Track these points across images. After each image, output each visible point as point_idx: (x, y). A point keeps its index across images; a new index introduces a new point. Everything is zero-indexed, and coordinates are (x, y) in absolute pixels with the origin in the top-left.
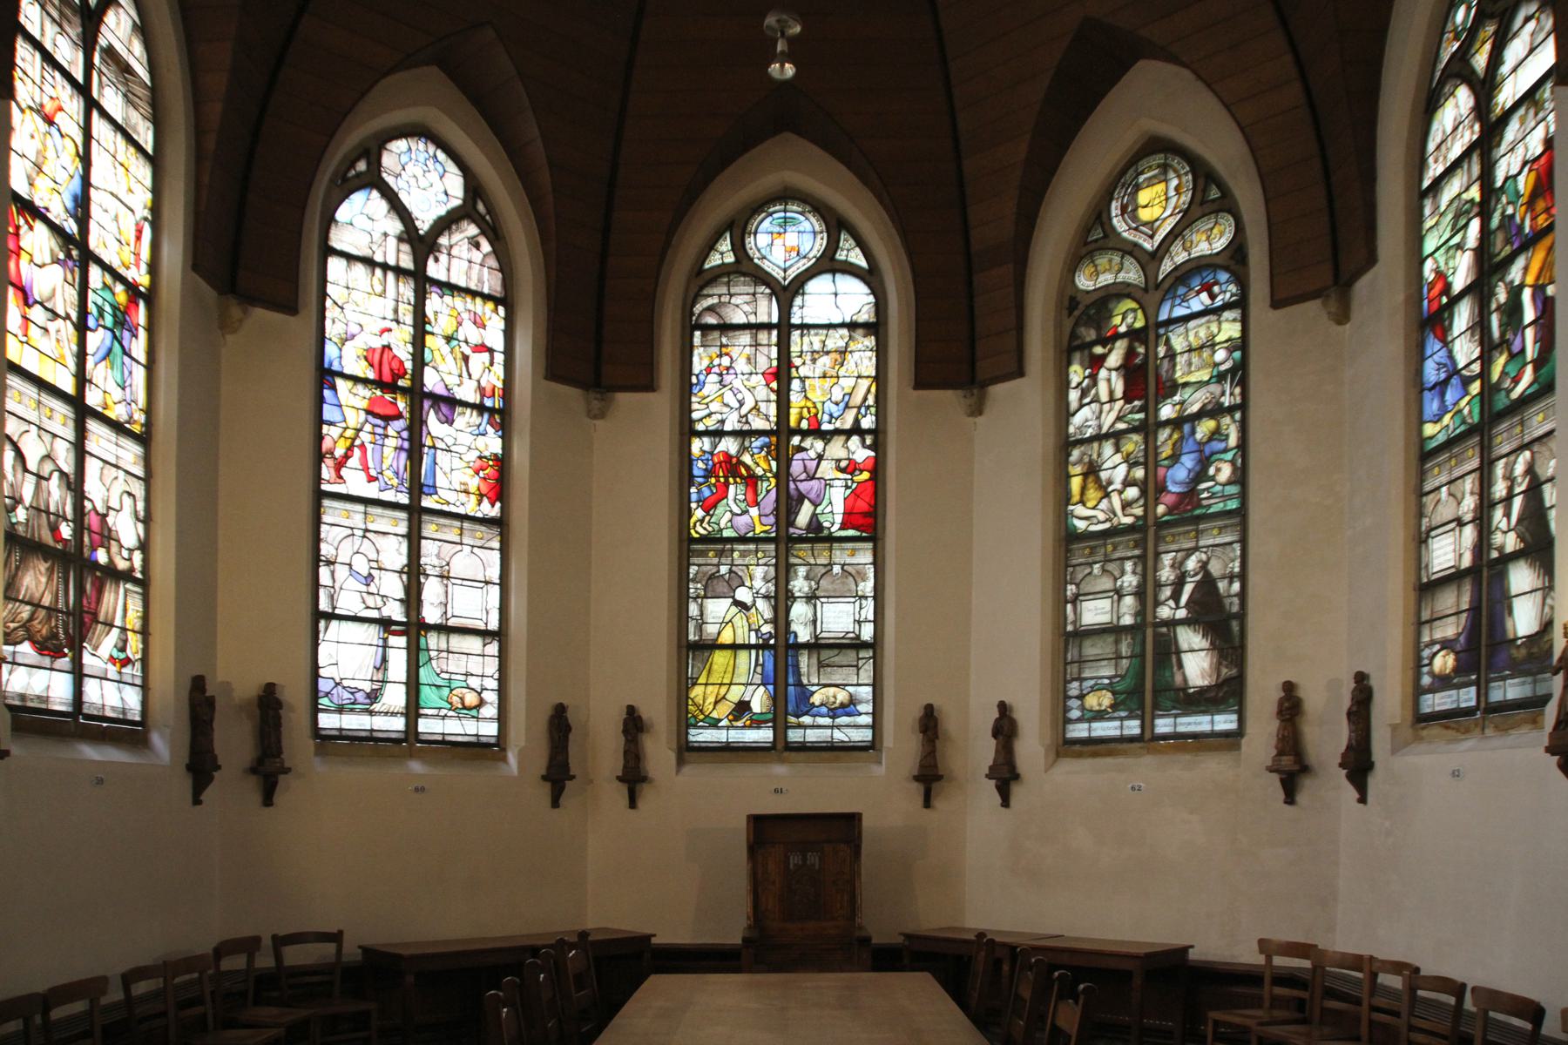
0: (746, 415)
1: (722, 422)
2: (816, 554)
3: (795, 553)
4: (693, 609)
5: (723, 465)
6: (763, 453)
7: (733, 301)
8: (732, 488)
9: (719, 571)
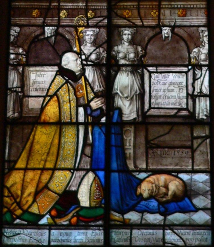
4: (13, 79)
9: (43, 33)
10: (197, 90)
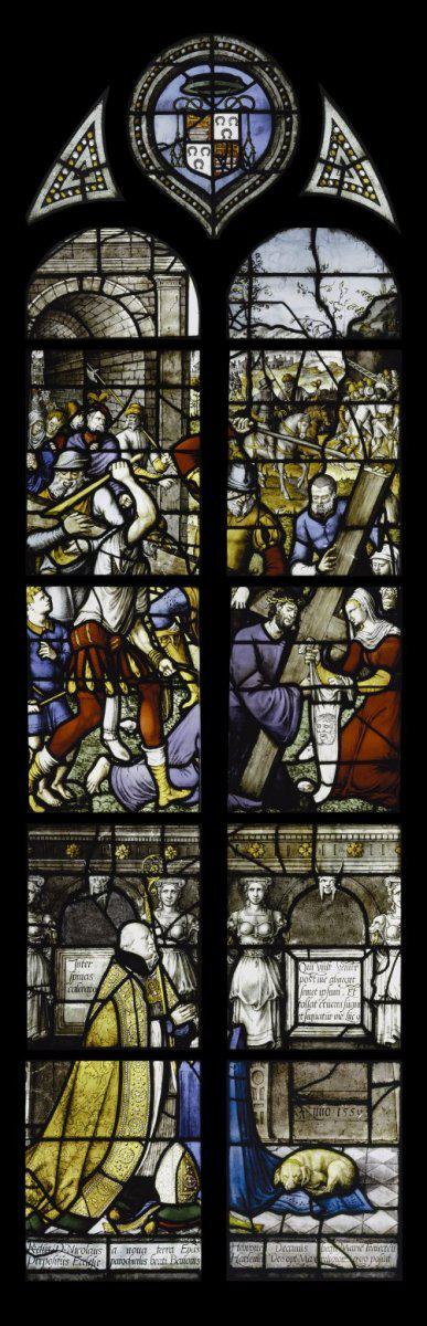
0: (138, 543)
1: (90, 557)
2: (284, 852)
3: (241, 848)
4: (35, 969)
5: (92, 651)
6: (174, 628)
7: (108, 288)
8: (110, 704)
9: (86, 886)
10: (381, 991)
